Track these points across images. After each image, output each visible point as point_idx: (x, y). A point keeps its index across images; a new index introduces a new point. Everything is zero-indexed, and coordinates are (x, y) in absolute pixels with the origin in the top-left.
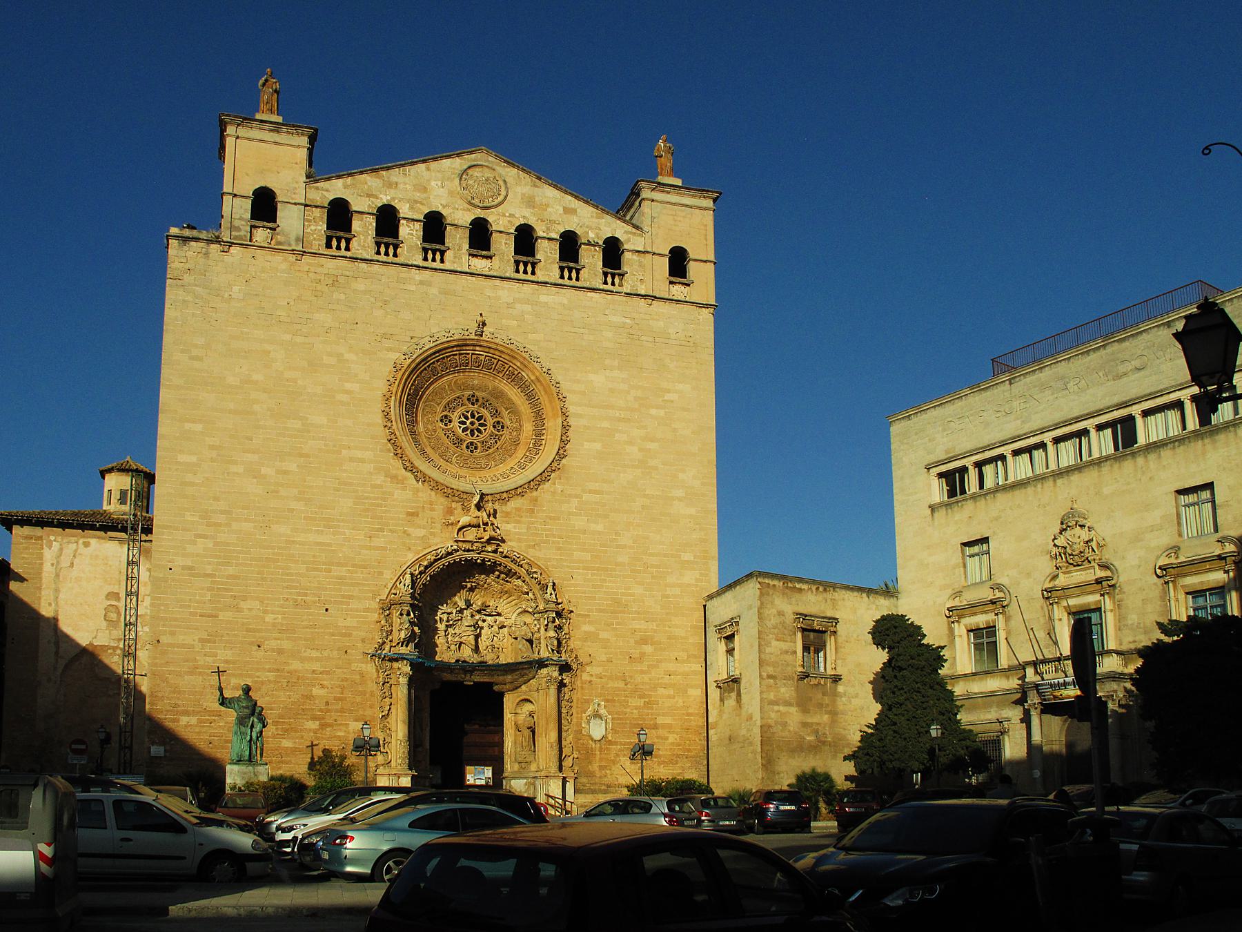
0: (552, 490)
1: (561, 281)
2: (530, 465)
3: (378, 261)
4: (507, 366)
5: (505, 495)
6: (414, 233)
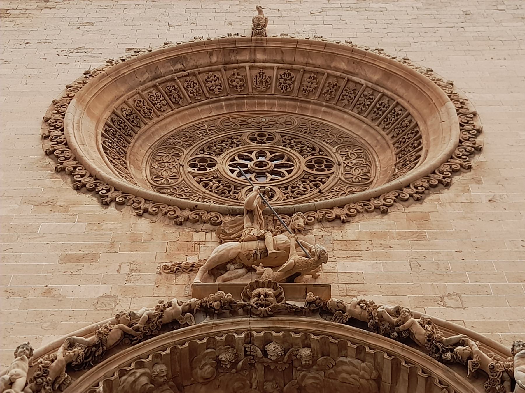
4: (322, 79)
5: (336, 211)
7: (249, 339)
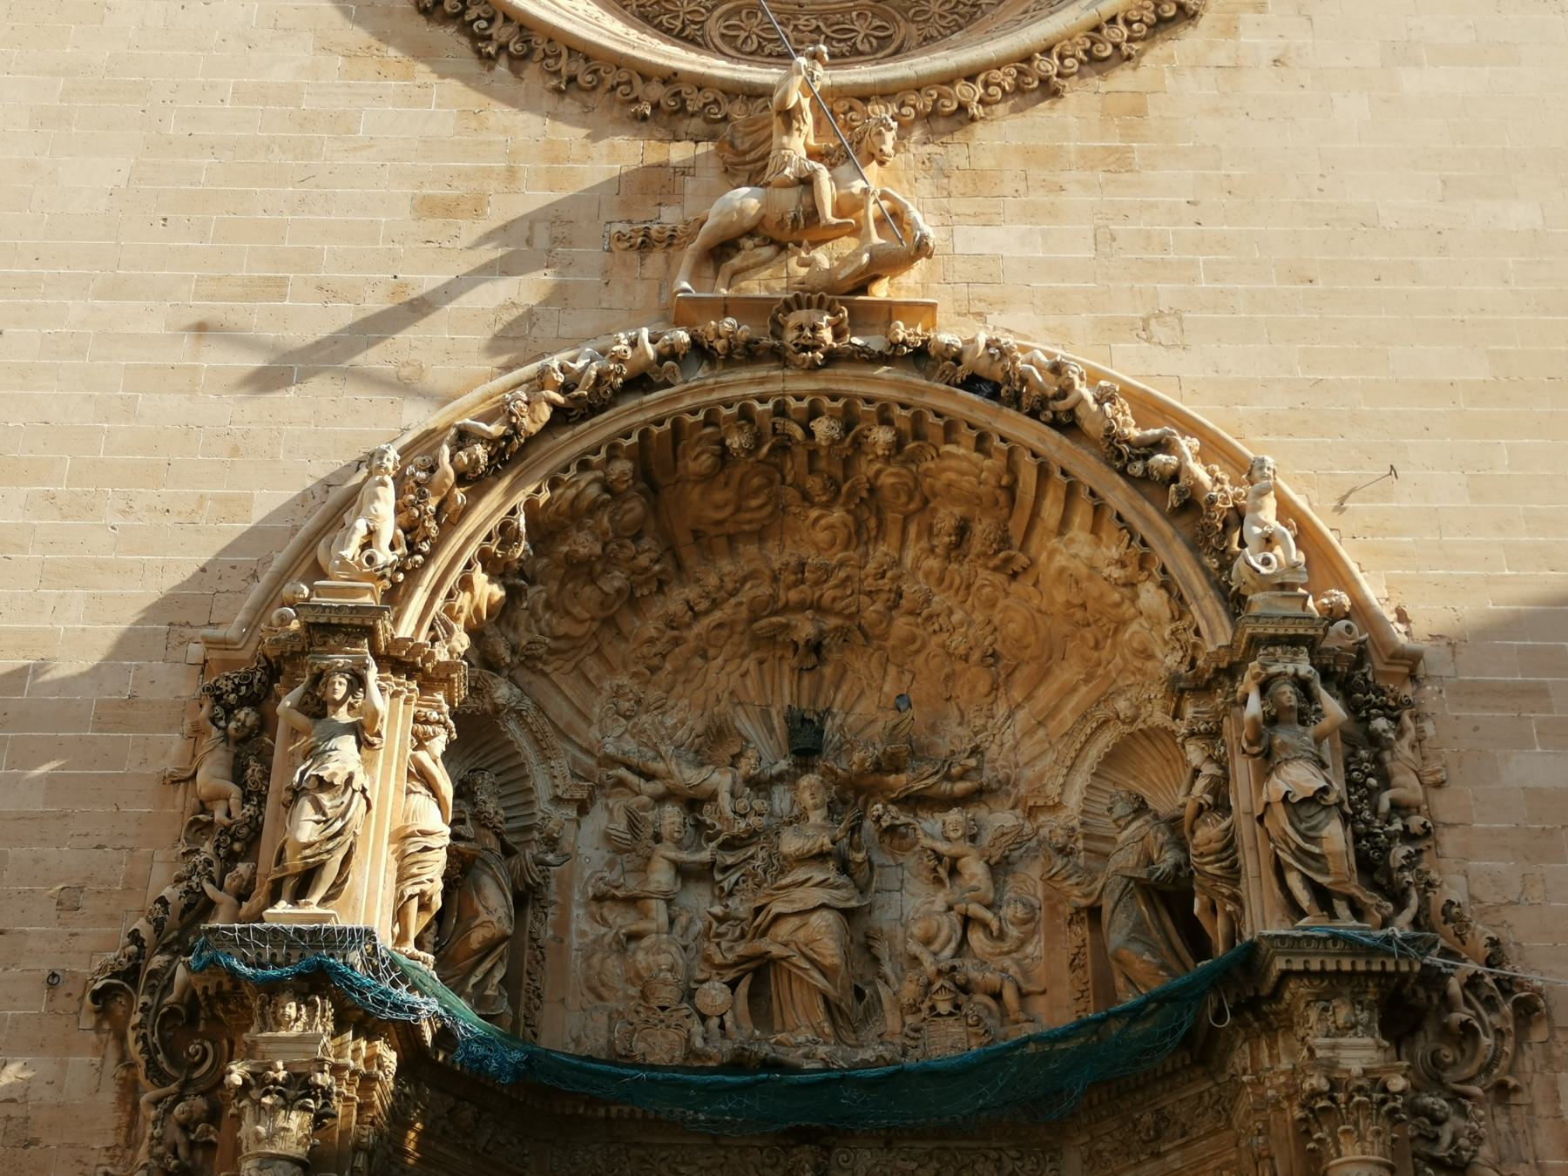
0: (1220, 56)
5: (962, 90)
7: (781, 410)
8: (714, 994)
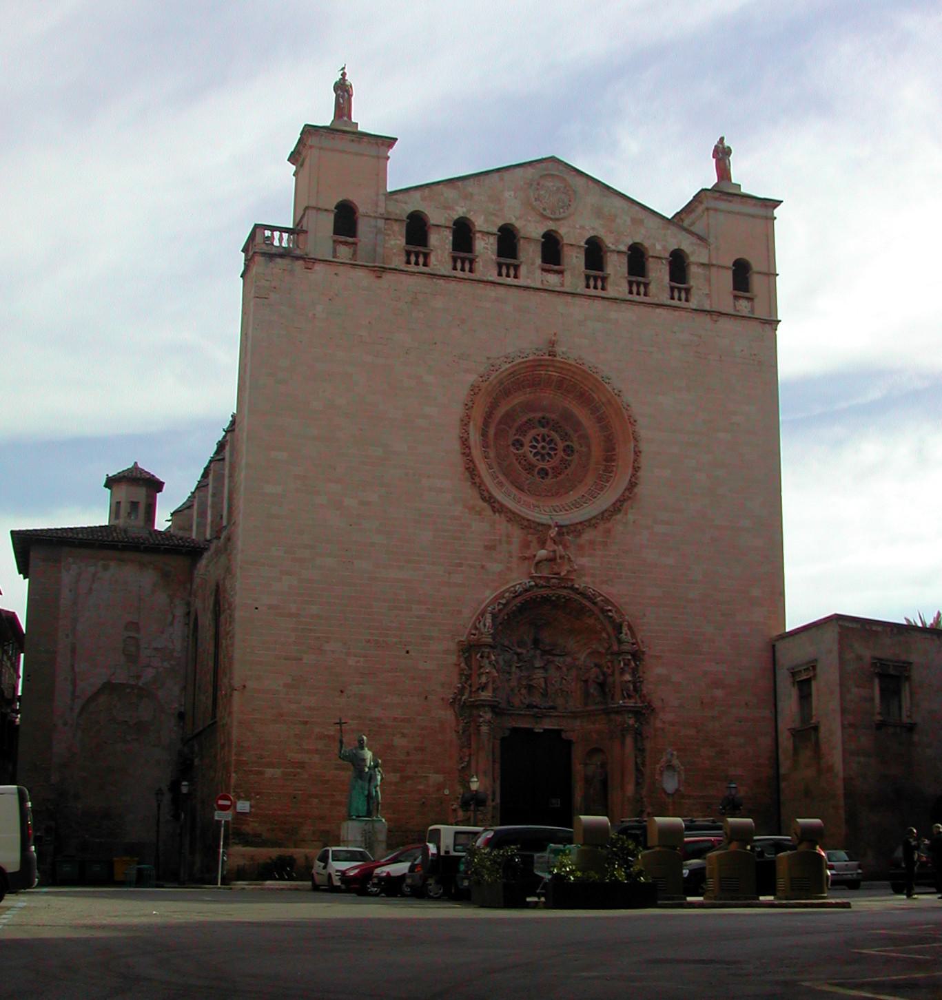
0: (624, 521)
1: (630, 297)
2: (602, 493)
3: (455, 277)
5: (579, 527)
6: (489, 246)
8: (524, 691)
